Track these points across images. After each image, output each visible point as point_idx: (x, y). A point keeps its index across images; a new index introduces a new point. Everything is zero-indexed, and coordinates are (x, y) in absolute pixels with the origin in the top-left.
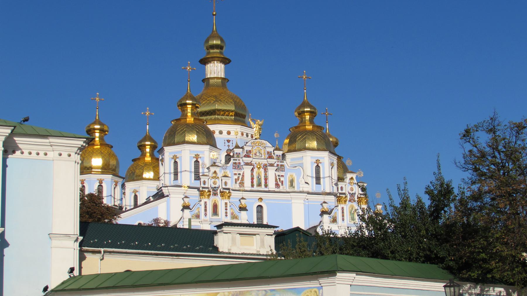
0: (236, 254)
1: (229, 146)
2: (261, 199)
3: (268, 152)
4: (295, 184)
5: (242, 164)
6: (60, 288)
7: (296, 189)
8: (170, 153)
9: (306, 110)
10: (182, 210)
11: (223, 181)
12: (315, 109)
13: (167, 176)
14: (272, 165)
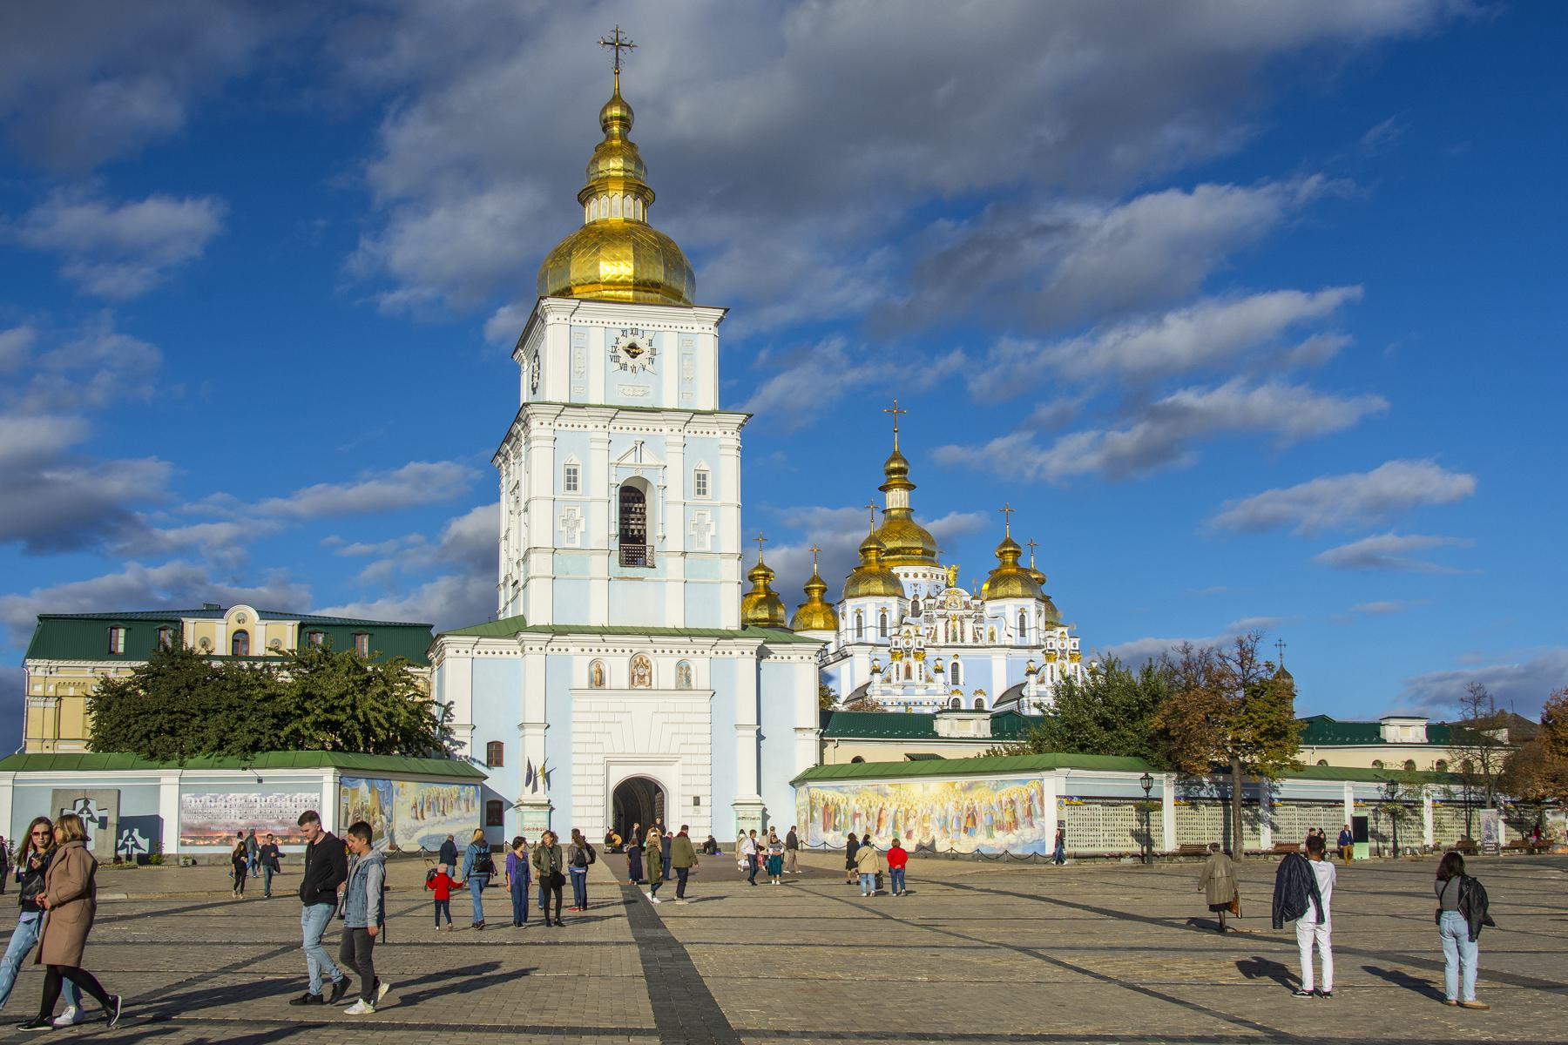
0: (955, 738)
1: (916, 591)
2: (956, 656)
3: (965, 602)
4: (996, 637)
5: (935, 616)
6: (813, 775)
7: (997, 644)
8: (853, 607)
9: (1008, 549)
10: (872, 674)
11: (917, 641)
12: (1019, 547)
13: (849, 632)
14: (969, 617)
